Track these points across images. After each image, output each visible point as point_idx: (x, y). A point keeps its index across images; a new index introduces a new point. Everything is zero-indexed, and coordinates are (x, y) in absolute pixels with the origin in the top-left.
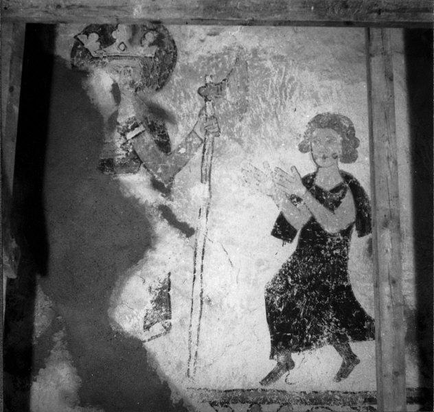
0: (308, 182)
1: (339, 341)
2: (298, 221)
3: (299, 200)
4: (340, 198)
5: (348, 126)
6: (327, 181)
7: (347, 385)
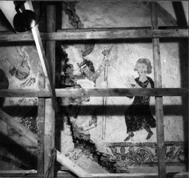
0: (137, 80)
3: (134, 86)
4: (147, 85)
5: (148, 62)
6: (143, 80)
7: (149, 141)
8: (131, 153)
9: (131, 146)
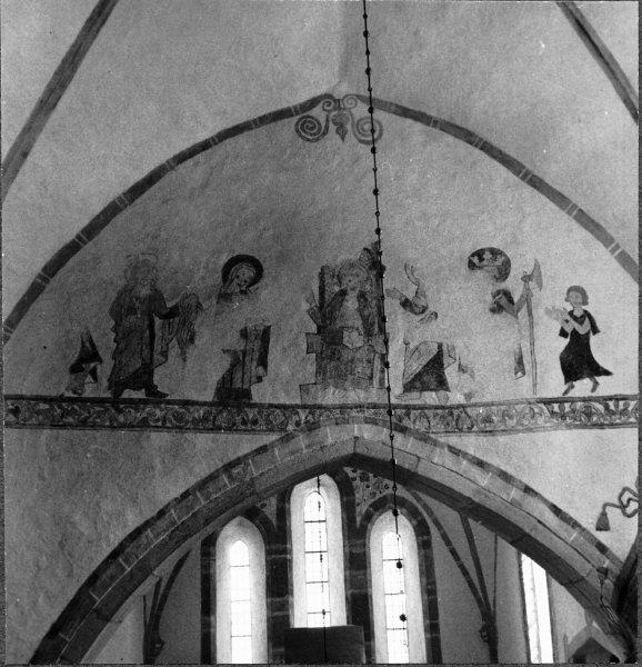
0: (571, 313)
2: (568, 329)
6: (578, 313)
7: (594, 394)
8: (573, 411)
9: (573, 401)
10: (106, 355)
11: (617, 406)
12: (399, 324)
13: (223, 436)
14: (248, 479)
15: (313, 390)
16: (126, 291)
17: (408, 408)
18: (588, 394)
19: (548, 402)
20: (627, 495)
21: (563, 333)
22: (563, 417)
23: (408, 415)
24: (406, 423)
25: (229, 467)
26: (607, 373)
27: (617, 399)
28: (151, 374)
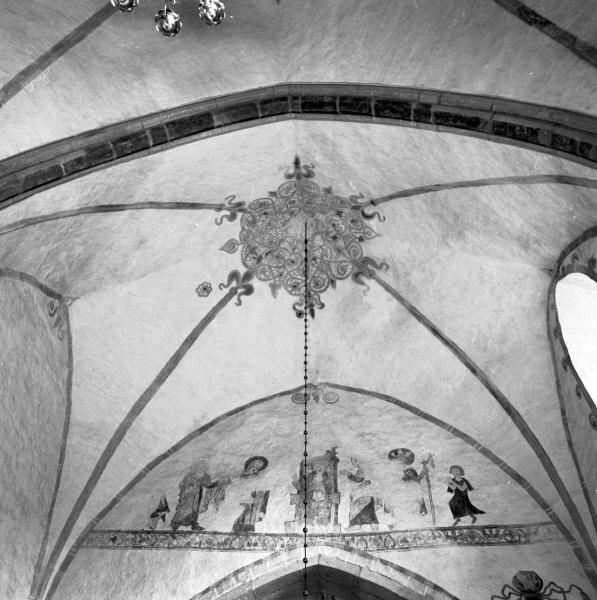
0: (454, 480)
1: (471, 514)
7: (476, 524)
9: (460, 528)
10: (173, 508)
11: (491, 532)
12: (346, 488)
13: (235, 554)
14: (248, 581)
15: (292, 525)
16: (191, 474)
17: (353, 535)
18: (469, 524)
19: (444, 529)
20: (507, 592)
21: (450, 490)
22: (455, 538)
23: (353, 540)
24: (352, 545)
25: (237, 573)
26: (482, 512)
27: (490, 527)
28: (196, 518)
